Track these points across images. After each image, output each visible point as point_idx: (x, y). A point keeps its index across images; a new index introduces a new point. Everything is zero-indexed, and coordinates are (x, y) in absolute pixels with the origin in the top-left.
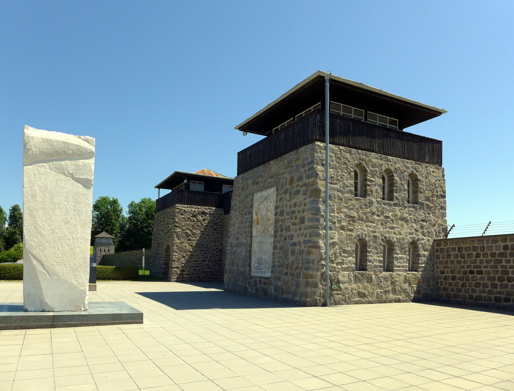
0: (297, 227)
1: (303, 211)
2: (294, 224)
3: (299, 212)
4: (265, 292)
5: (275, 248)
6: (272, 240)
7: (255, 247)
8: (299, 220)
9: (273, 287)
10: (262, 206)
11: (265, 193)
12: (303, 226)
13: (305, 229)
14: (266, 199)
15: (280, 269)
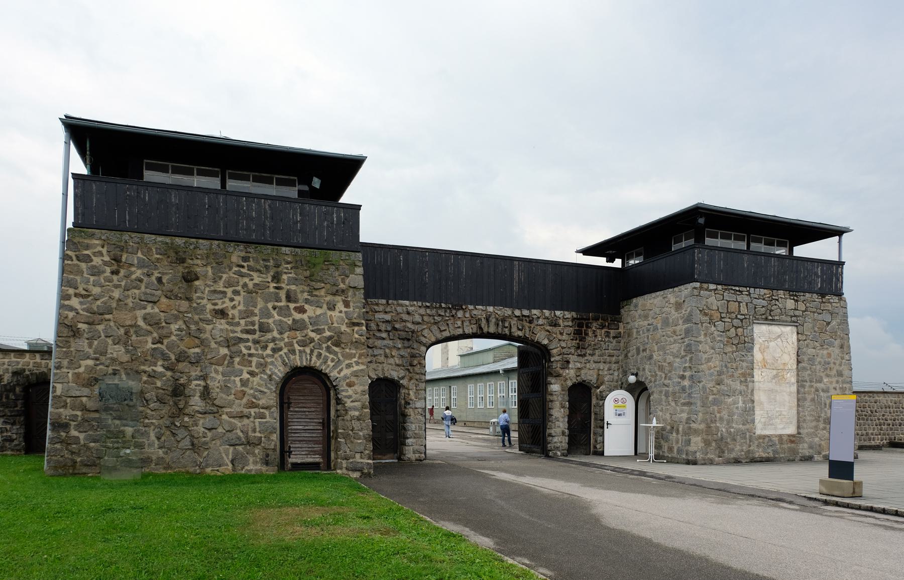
0: (834, 380)
1: (840, 365)
2: (828, 376)
3: (835, 363)
4: (794, 452)
5: (800, 401)
6: (794, 388)
7: (760, 396)
8: (834, 372)
9: (806, 445)
10: (772, 344)
11: (776, 329)
12: (840, 379)
13: (843, 382)
14: (779, 336)
15: (814, 424)
